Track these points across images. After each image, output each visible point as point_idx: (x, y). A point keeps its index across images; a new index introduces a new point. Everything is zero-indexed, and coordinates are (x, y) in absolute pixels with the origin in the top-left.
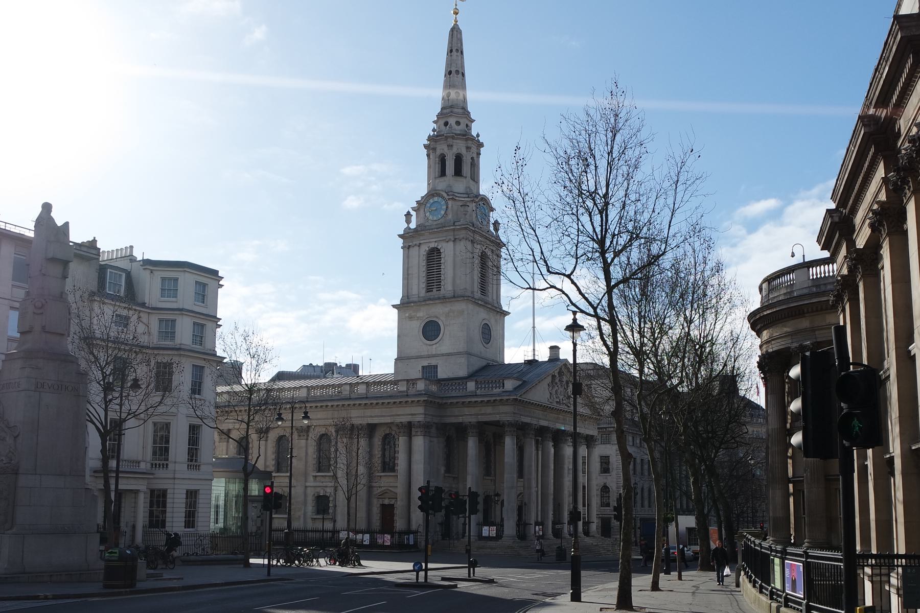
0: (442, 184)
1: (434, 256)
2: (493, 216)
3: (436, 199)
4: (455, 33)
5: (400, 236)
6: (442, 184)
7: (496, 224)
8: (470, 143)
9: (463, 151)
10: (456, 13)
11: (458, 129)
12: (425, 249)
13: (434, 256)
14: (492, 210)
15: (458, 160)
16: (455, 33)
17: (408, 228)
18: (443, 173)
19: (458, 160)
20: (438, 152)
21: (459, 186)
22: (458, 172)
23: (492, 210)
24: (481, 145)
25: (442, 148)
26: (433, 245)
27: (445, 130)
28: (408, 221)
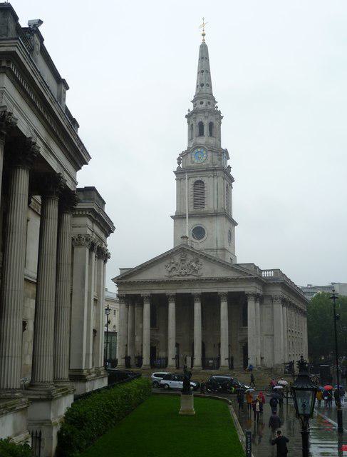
0: (202, 141)
1: (199, 185)
2: (229, 163)
3: (199, 150)
4: (204, 49)
5: (174, 172)
6: (202, 141)
7: (229, 167)
8: (218, 116)
9: (213, 120)
10: (204, 35)
11: (210, 107)
12: (193, 180)
13: (199, 185)
14: (229, 158)
15: (211, 125)
16: (204, 49)
17: (179, 168)
18: (201, 133)
19: (211, 125)
20: (198, 121)
21: (212, 141)
22: (211, 135)
23: (229, 158)
24: (222, 117)
25: (201, 118)
26: (198, 179)
27: (200, 106)
28: (179, 163)
